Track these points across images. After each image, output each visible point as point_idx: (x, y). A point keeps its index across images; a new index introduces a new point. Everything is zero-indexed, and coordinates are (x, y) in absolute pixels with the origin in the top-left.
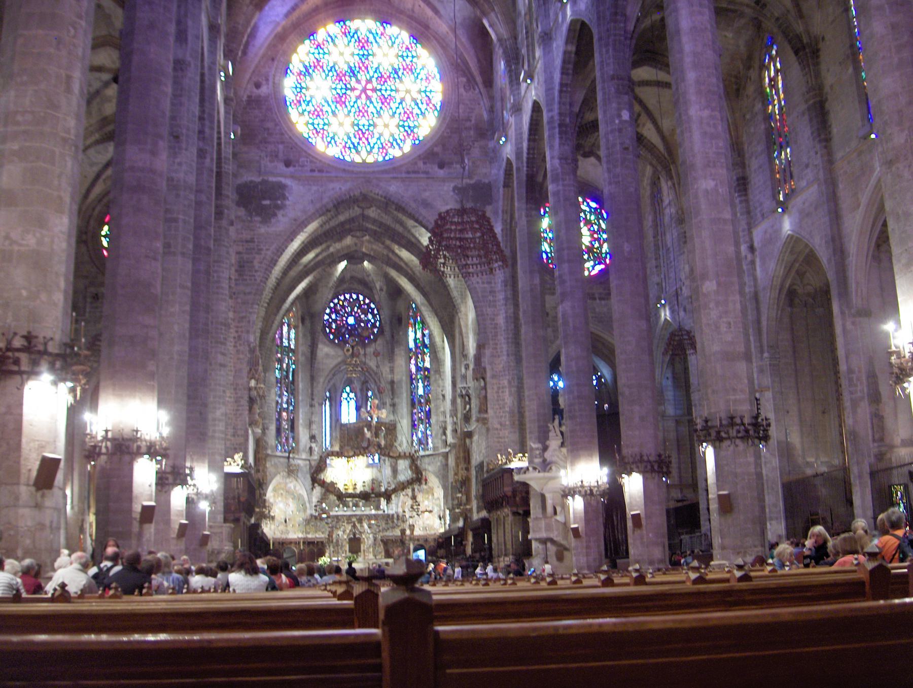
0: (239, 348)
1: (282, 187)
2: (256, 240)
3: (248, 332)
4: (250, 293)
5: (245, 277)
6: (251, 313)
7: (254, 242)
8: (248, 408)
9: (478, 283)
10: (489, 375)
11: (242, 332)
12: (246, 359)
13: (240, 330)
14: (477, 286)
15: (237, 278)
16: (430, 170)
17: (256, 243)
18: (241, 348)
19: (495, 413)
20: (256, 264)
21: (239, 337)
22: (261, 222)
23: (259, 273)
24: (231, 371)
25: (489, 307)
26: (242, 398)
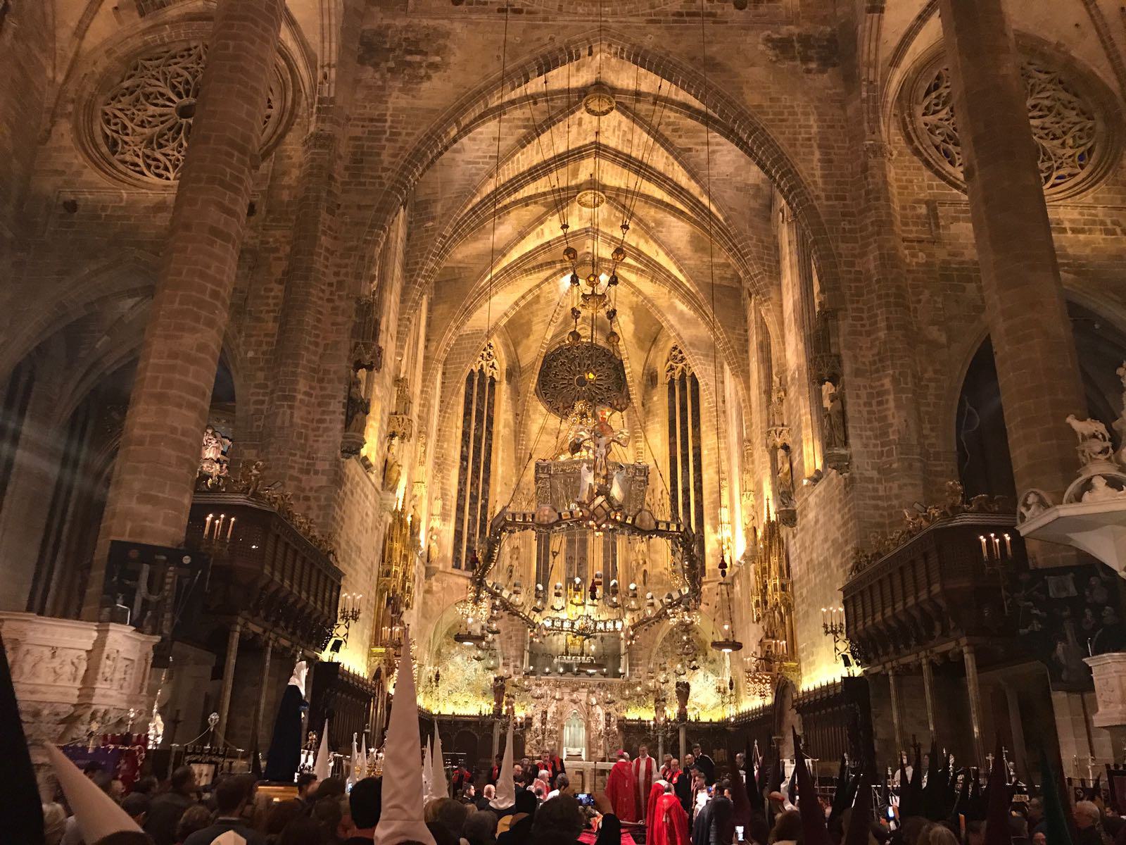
0: (337, 303)
1: (447, 35)
2: (389, 119)
3: (358, 276)
4: (369, 207)
5: (363, 180)
6: (366, 242)
7: (385, 121)
8: (343, 417)
9: (818, 198)
10: (847, 368)
11: (346, 274)
12: (350, 325)
13: (343, 271)
14: (815, 203)
15: (347, 180)
16: (719, 12)
17: (388, 124)
18: (343, 304)
19: (866, 446)
20: (386, 158)
21: (340, 283)
22: (401, 90)
23: (389, 173)
24: (317, 345)
25: (843, 242)
26: (334, 397)
